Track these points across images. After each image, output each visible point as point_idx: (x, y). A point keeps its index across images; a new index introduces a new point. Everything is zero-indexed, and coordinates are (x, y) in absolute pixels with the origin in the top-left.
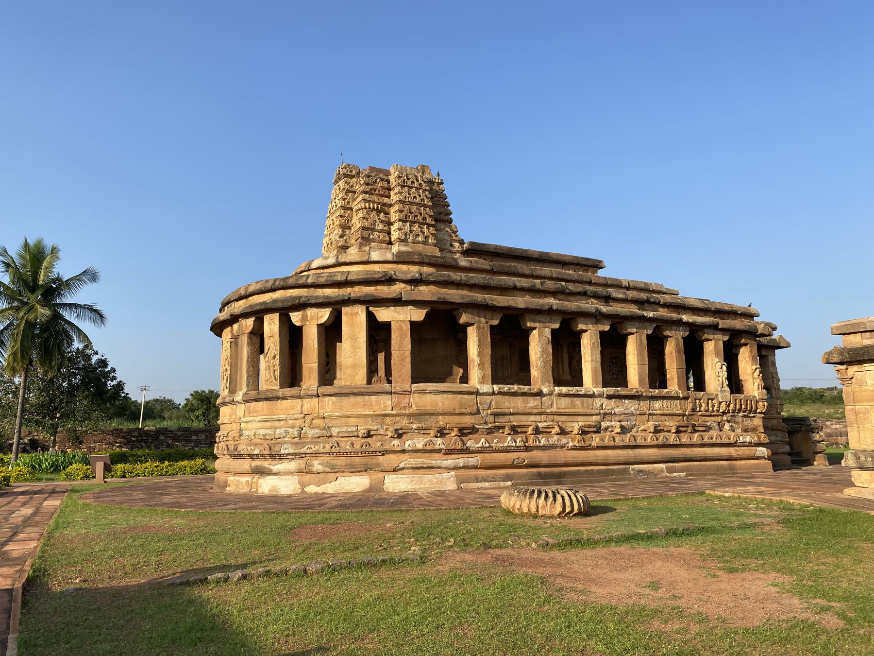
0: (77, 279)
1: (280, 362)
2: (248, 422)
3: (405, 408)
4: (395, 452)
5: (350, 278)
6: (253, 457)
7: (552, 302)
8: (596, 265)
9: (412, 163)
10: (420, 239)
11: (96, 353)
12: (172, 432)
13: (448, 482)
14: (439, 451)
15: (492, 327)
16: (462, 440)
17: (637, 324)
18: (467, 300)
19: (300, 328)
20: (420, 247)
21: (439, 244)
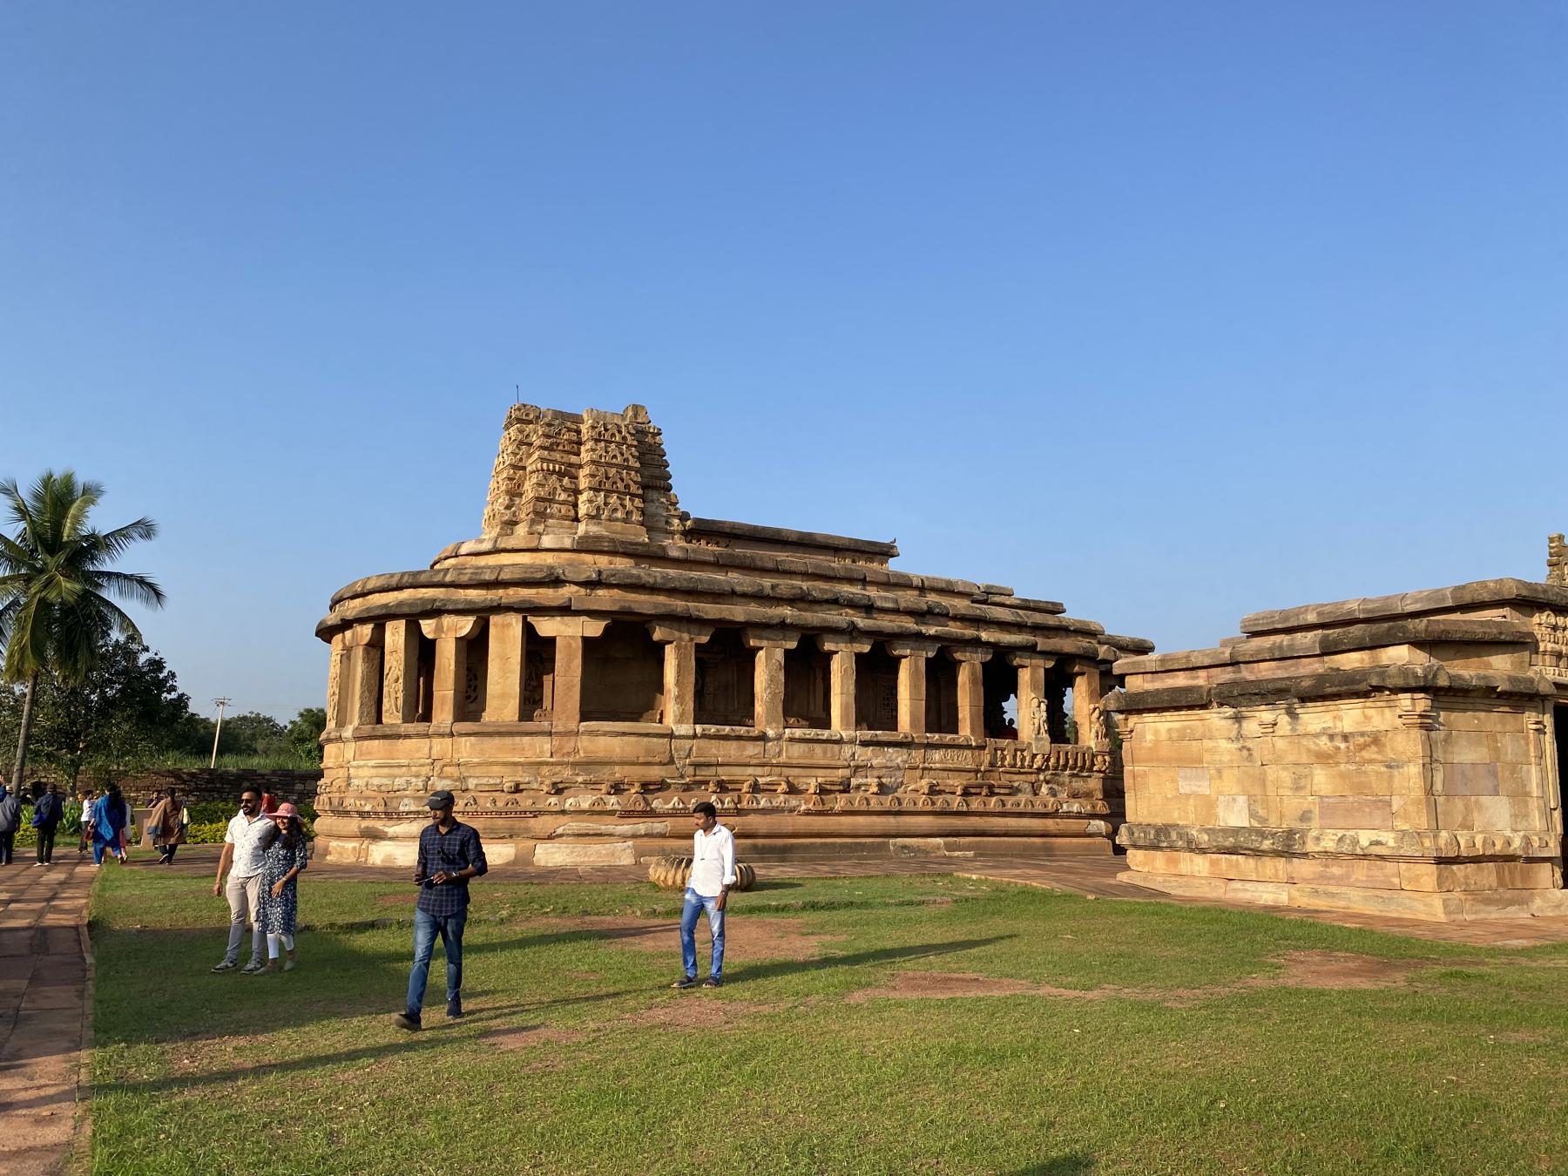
0: (123, 533)
1: (405, 689)
2: (358, 767)
3: (569, 754)
4: (552, 813)
5: (505, 576)
6: (363, 815)
7: (787, 612)
8: (884, 552)
9: (614, 404)
10: (619, 515)
11: (146, 649)
12: (263, 776)
13: (622, 855)
14: (612, 813)
17: (912, 644)
18: (662, 610)
19: (433, 642)
20: (619, 526)
21: (649, 524)
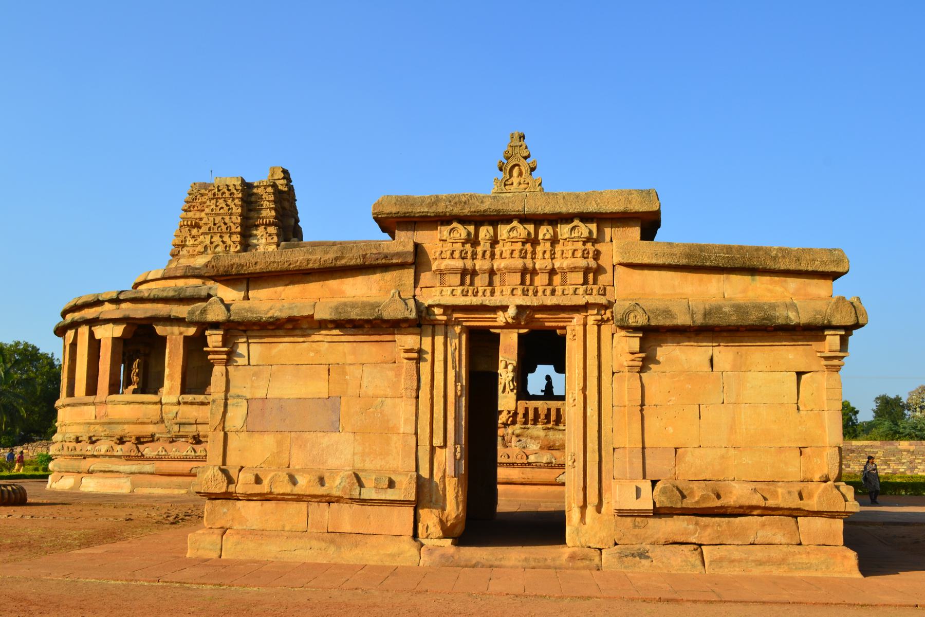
15: (186, 338)
16: (138, 448)
